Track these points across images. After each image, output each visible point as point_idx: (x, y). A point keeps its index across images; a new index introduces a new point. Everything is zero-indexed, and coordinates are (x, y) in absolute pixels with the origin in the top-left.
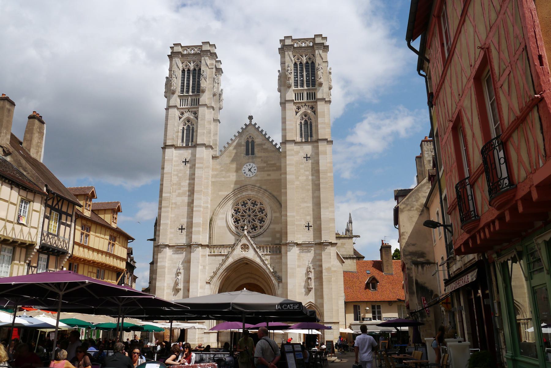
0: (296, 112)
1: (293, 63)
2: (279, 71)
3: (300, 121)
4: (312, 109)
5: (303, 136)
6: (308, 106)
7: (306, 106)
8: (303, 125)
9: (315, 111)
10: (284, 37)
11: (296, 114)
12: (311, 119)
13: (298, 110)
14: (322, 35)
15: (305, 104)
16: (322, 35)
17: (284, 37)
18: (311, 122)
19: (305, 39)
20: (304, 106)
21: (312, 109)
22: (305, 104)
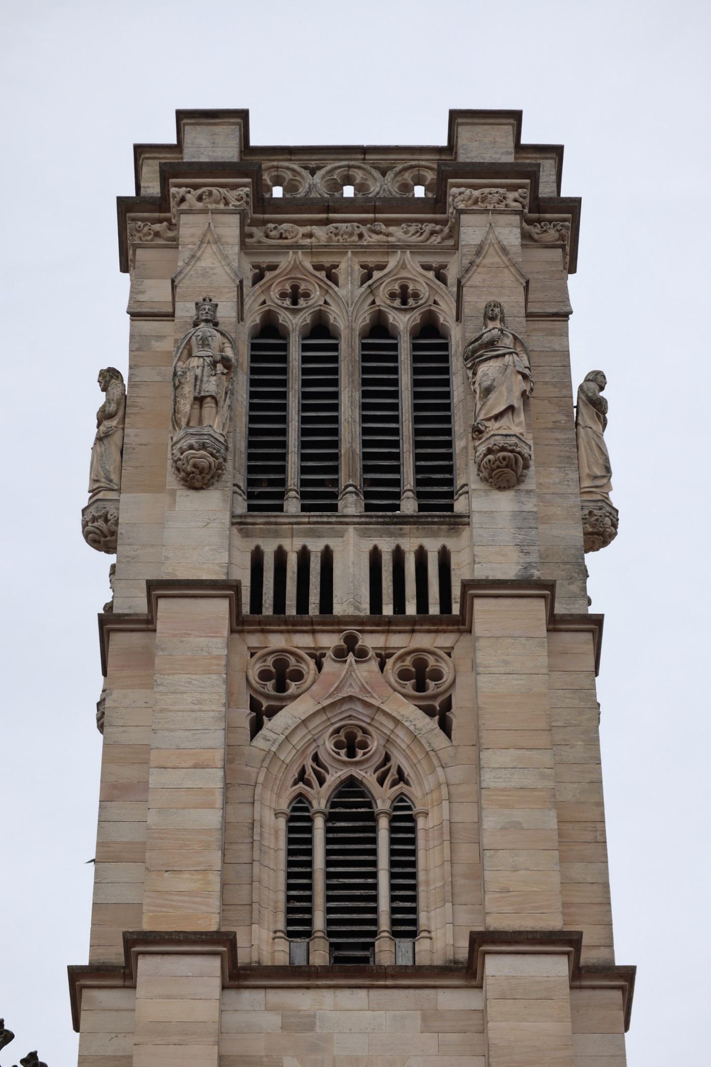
0: (254, 705)
1: (254, 318)
2: (109, 377)
3: (291, 792)
4: (420, 687)
5: (319, 921)
6: (374, 665)
7: (362, 655)
8: (319, 824)
9: (447, 705)
10: (181, 115)
11: (256, 727)
12: (401, 777)
13: (281, 687)
14: (516, 117)
15: (351, 641)
16: (516, 117)
17: (181, 115)
18: (401, 797)
19: (364, 150)
20: (340, 654)
21: (420, 687)
22: (351, 641)
